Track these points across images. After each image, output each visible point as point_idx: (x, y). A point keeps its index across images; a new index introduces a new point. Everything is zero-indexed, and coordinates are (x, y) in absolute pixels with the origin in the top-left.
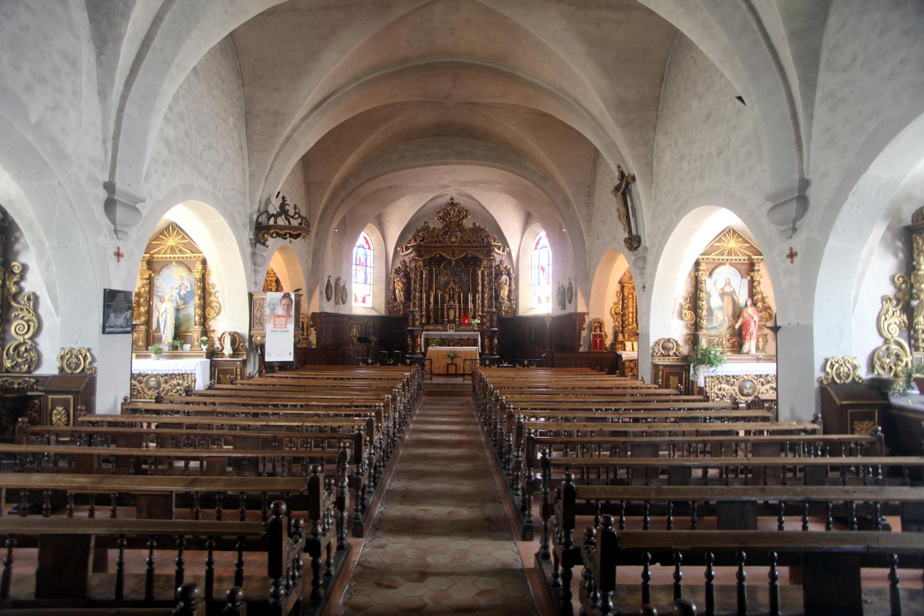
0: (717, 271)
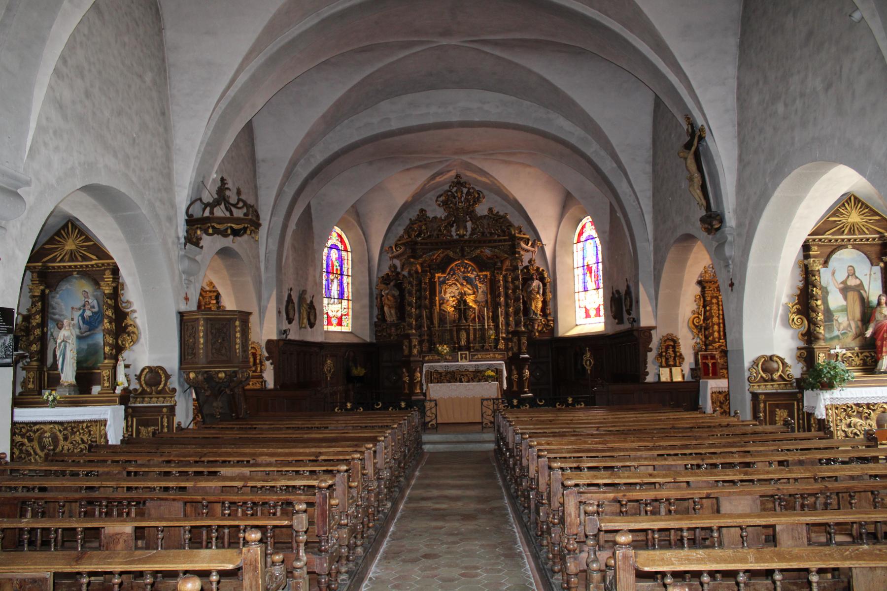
0: (835, 256)
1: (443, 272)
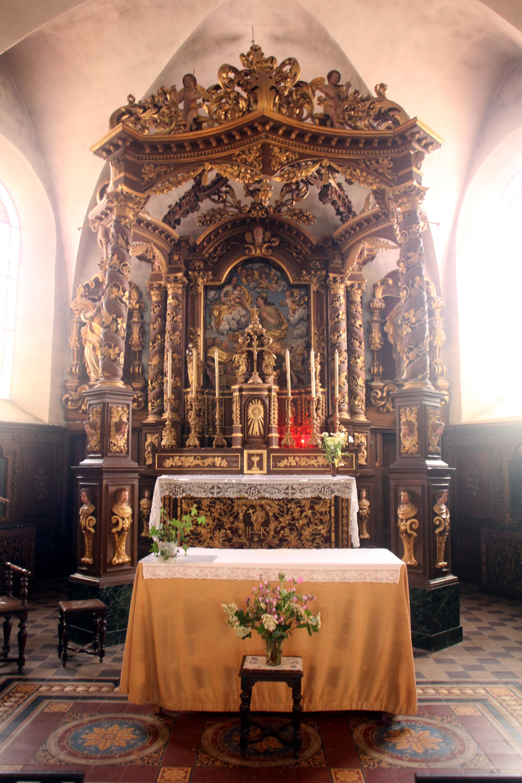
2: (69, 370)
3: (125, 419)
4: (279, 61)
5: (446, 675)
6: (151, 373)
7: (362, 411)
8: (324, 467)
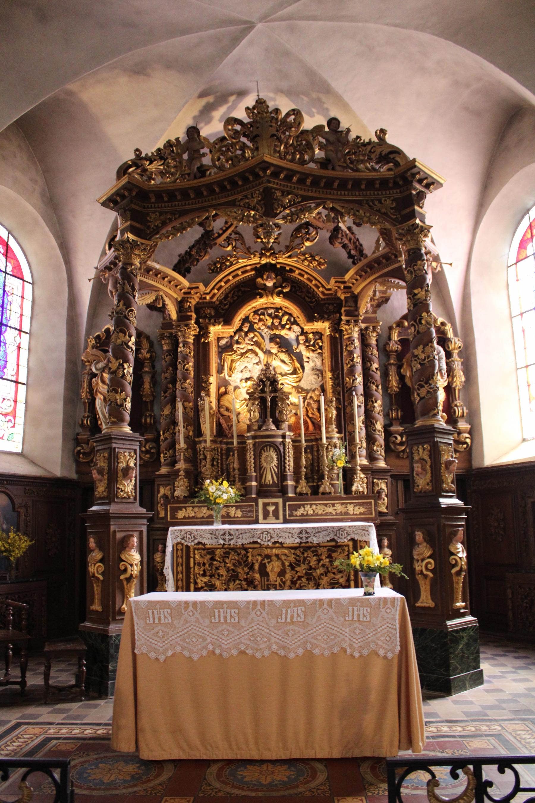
1: (228, 322)
2: (80, 422)
3: (132, 465)
4: (284, 113)
5: (463, 715)
6: (163, 422)
7: (381, 457)
8: (342, 515)
